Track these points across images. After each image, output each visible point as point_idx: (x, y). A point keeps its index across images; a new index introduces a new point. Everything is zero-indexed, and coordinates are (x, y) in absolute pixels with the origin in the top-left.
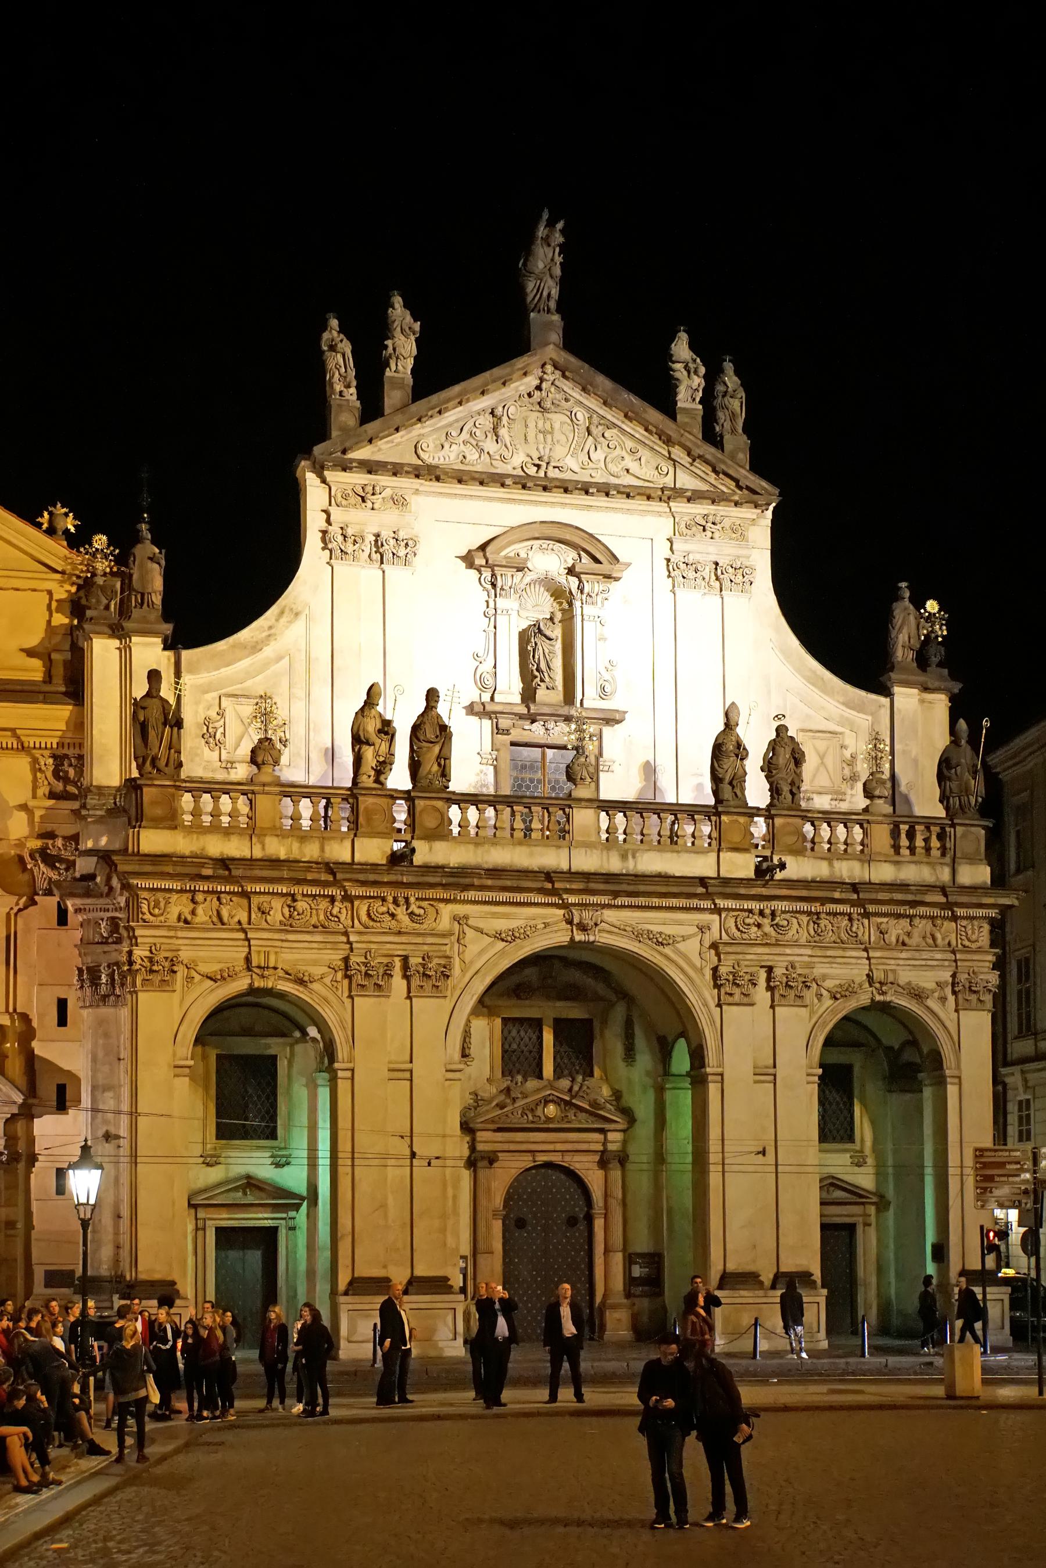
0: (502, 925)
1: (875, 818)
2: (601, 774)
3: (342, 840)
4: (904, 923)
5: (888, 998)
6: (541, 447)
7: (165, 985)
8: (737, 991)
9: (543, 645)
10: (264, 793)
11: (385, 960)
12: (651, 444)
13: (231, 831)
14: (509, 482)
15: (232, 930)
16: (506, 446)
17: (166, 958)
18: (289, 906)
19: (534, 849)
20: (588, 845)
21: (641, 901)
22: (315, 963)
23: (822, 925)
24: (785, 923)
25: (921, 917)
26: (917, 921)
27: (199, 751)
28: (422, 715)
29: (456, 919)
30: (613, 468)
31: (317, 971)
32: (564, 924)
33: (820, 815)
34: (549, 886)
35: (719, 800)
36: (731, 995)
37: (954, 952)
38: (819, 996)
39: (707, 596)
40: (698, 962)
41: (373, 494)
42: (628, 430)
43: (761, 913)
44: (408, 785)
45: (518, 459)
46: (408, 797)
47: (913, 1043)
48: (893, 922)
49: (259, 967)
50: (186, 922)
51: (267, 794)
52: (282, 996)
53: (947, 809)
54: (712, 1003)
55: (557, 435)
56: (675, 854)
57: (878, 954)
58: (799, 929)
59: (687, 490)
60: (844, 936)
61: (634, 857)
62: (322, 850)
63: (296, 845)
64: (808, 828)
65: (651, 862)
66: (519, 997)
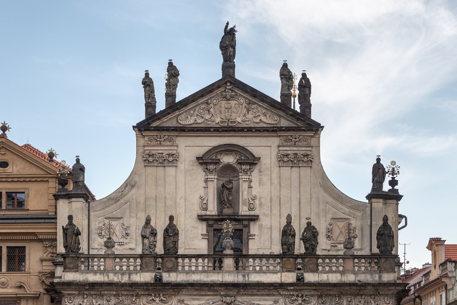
1: (346, 257)
2: (250, 241)
3: (137, 273)
4: (359, 297)
6: (226, 114)
9: (226, 192)
10: (108, 258)
12: (270, 109)
13: (97, 272)
14: (212, 130)
16: (212, 115)
18: (118, 299)
19: (209, 274)
20: (229, 272)
21: (250, 292)
23: (324, 299)
24: (308, 299)
25: (366, 295)
26: (363, 297)
27: (96, 239)
28: (169, 225)
33: (324, 256)
34: (213, 288)
35: (283, 253)
39: (293, 169)
41: (160, 138)
42: (261, 104)
43: (297, 296)
44: (163, 252)
45: (218, 120)
46: (161, 256)
48: (353, 297)
51: (110, 258)
53: (380, 251)
55: (233, 109)
56: (265, 274)
59: (283, 127)
61: (248, 276)
62: (129, 277)
63: (120, 276)
65: (254, 278)
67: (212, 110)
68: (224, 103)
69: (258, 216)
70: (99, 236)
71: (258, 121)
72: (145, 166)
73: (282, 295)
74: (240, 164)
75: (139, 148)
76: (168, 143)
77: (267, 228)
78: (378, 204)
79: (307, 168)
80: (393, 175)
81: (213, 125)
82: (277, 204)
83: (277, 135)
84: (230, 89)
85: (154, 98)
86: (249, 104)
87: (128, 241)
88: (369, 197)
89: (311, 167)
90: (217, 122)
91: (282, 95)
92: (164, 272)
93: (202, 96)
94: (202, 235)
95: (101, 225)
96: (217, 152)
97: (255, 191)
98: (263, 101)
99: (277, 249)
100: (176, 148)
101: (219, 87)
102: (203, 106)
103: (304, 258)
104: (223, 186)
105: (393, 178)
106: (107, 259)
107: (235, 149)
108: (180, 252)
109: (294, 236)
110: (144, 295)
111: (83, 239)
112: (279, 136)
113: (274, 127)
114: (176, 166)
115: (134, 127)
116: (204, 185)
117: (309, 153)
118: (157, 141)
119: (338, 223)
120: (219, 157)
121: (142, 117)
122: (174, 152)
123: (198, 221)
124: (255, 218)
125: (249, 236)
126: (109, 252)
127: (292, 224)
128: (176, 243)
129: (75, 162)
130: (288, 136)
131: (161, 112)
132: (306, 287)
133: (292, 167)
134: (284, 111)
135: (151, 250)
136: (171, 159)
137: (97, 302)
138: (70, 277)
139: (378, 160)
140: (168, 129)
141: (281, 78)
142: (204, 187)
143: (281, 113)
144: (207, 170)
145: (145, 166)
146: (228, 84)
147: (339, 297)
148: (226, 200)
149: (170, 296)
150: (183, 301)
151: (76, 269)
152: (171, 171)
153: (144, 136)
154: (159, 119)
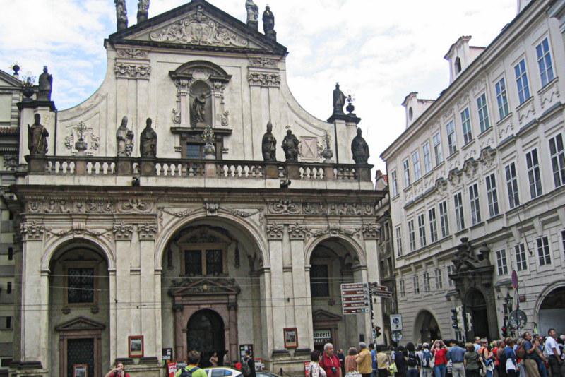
0: (177, 210)
4: (341, 206)
5: (335, 235)
7: (38, 240)
8: (275, 235)
11: (128, 226)
15: (65, 215)
16: (184, 35)
17: (38, 227)
22: (103, 228)
26: (346, 205)
29: (159, 208)
30: (225, 42)
31: (101, 231)
32: (203, 210)
36: (273, 236)
37: (362, 216)
38: (309, 235)
39: (263, 89)
40: (259, 223)
43: (283, 203)
44: (139, 155)
45: (189, 40)
46: (138, 160)
47: (348, 254)
49: (76, 230)
50: (46, 212)
51: (82, 160)
52: (88, 241)
54: (265, 240)
55: (204, 31)
57: (331, 218)
58: (299, 210)
60: (317, 212)
64: (301, 170)
66: (192, 242)
67: (184, 30)
68: (195, 25)
69: (231, 130)
70: (67, 146)
71: (228, 43)
72: (117, 78)
73: (266, 203)
74: (212, 80)
75: (110, 61)
76: (140, 57)
77: (240, 144)
78: (341, 125)
79: (275, 89)
80: (349, 101)
81: (186, 43)
82: (249, 121)
83: (245, 56)
84: (201, 12)
85: (125, 15)
86: (218, 27)
87: (97, 152)
88: (331, 120)
89: (279, 88)
90: (188, 41)
91: (249, 22)
92: (143, 176)
93: (175, 16)
94: (175, 148)
95: (69, 135)
96: (189, 68)
97: (226, 108)
98: (232, 25)
99: (259, 157)
100: (148, 62)
101: (190, 9)
102: (174, 26)
103: (287, 165)
104: (196, 100)
105: (350, 104)
106: (78, 162)
107: (208, 66)
108: (159, 155)
109: (275, 143)
110: (118, 201)
111: (50, 140)
112: (248, 58)
113: (244, 48)
114: (148, 80)
115: (105, 40)
116: (177, 99)
117: (277, 75)
118: (129, 54)
119: (307, 141)
120: (191, 73)
121: (114, 30)
122: (147, 66)
123: (171, 134)
124: (228, 133)
125: (223, 150)
126: (81, 154)
127: (272, 132)
128: (154, 147)
129: (43, 72)
130: (256, 58)
131: (134, 27)
132: (292, 194)
133: (261, 87)
134: (253, 35)
135: (128, 153)
136: (143, 72)
137: (65, 209)
138: (34, 180)
139: (338, 86)
140: (141, 43)
141: (247, 9)
142: (177, 102)
143: (250, 37)
144: (179, 85)
145: (117, 78)
146: (200, 7)
147: (322, 204)
148: (199, 113)
149: (148, 201)
150: (163, 208)
151: (43, 172)
152: (142, 84)
153: (116, 50)
154: (131, 33)
